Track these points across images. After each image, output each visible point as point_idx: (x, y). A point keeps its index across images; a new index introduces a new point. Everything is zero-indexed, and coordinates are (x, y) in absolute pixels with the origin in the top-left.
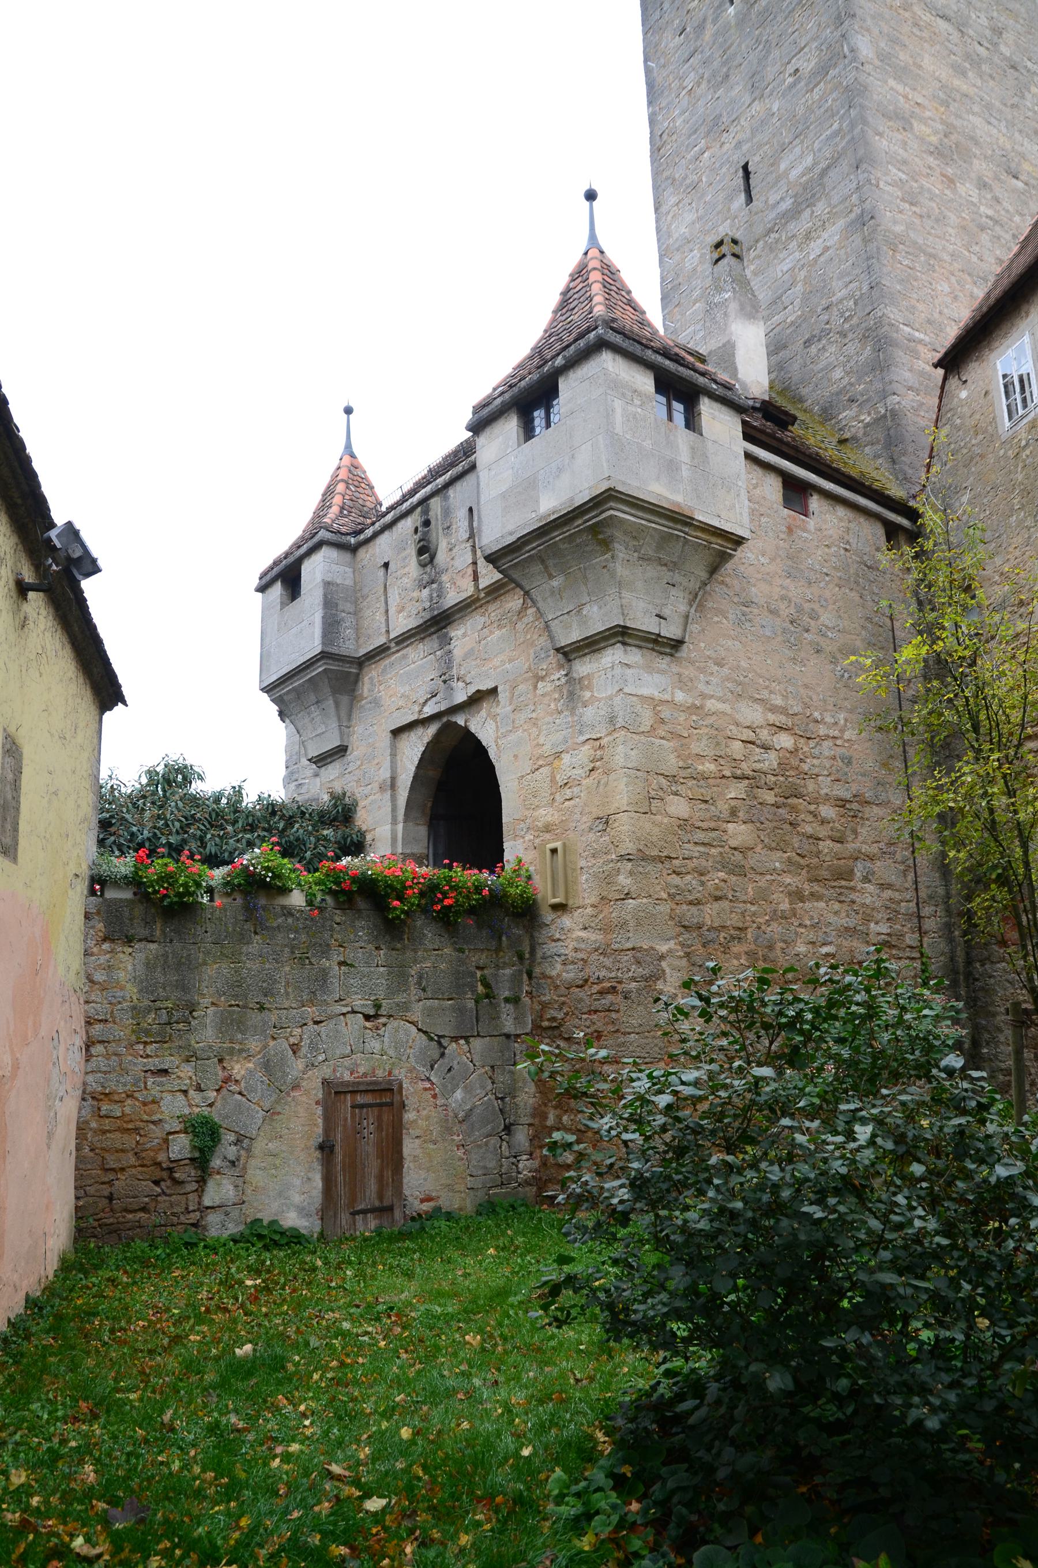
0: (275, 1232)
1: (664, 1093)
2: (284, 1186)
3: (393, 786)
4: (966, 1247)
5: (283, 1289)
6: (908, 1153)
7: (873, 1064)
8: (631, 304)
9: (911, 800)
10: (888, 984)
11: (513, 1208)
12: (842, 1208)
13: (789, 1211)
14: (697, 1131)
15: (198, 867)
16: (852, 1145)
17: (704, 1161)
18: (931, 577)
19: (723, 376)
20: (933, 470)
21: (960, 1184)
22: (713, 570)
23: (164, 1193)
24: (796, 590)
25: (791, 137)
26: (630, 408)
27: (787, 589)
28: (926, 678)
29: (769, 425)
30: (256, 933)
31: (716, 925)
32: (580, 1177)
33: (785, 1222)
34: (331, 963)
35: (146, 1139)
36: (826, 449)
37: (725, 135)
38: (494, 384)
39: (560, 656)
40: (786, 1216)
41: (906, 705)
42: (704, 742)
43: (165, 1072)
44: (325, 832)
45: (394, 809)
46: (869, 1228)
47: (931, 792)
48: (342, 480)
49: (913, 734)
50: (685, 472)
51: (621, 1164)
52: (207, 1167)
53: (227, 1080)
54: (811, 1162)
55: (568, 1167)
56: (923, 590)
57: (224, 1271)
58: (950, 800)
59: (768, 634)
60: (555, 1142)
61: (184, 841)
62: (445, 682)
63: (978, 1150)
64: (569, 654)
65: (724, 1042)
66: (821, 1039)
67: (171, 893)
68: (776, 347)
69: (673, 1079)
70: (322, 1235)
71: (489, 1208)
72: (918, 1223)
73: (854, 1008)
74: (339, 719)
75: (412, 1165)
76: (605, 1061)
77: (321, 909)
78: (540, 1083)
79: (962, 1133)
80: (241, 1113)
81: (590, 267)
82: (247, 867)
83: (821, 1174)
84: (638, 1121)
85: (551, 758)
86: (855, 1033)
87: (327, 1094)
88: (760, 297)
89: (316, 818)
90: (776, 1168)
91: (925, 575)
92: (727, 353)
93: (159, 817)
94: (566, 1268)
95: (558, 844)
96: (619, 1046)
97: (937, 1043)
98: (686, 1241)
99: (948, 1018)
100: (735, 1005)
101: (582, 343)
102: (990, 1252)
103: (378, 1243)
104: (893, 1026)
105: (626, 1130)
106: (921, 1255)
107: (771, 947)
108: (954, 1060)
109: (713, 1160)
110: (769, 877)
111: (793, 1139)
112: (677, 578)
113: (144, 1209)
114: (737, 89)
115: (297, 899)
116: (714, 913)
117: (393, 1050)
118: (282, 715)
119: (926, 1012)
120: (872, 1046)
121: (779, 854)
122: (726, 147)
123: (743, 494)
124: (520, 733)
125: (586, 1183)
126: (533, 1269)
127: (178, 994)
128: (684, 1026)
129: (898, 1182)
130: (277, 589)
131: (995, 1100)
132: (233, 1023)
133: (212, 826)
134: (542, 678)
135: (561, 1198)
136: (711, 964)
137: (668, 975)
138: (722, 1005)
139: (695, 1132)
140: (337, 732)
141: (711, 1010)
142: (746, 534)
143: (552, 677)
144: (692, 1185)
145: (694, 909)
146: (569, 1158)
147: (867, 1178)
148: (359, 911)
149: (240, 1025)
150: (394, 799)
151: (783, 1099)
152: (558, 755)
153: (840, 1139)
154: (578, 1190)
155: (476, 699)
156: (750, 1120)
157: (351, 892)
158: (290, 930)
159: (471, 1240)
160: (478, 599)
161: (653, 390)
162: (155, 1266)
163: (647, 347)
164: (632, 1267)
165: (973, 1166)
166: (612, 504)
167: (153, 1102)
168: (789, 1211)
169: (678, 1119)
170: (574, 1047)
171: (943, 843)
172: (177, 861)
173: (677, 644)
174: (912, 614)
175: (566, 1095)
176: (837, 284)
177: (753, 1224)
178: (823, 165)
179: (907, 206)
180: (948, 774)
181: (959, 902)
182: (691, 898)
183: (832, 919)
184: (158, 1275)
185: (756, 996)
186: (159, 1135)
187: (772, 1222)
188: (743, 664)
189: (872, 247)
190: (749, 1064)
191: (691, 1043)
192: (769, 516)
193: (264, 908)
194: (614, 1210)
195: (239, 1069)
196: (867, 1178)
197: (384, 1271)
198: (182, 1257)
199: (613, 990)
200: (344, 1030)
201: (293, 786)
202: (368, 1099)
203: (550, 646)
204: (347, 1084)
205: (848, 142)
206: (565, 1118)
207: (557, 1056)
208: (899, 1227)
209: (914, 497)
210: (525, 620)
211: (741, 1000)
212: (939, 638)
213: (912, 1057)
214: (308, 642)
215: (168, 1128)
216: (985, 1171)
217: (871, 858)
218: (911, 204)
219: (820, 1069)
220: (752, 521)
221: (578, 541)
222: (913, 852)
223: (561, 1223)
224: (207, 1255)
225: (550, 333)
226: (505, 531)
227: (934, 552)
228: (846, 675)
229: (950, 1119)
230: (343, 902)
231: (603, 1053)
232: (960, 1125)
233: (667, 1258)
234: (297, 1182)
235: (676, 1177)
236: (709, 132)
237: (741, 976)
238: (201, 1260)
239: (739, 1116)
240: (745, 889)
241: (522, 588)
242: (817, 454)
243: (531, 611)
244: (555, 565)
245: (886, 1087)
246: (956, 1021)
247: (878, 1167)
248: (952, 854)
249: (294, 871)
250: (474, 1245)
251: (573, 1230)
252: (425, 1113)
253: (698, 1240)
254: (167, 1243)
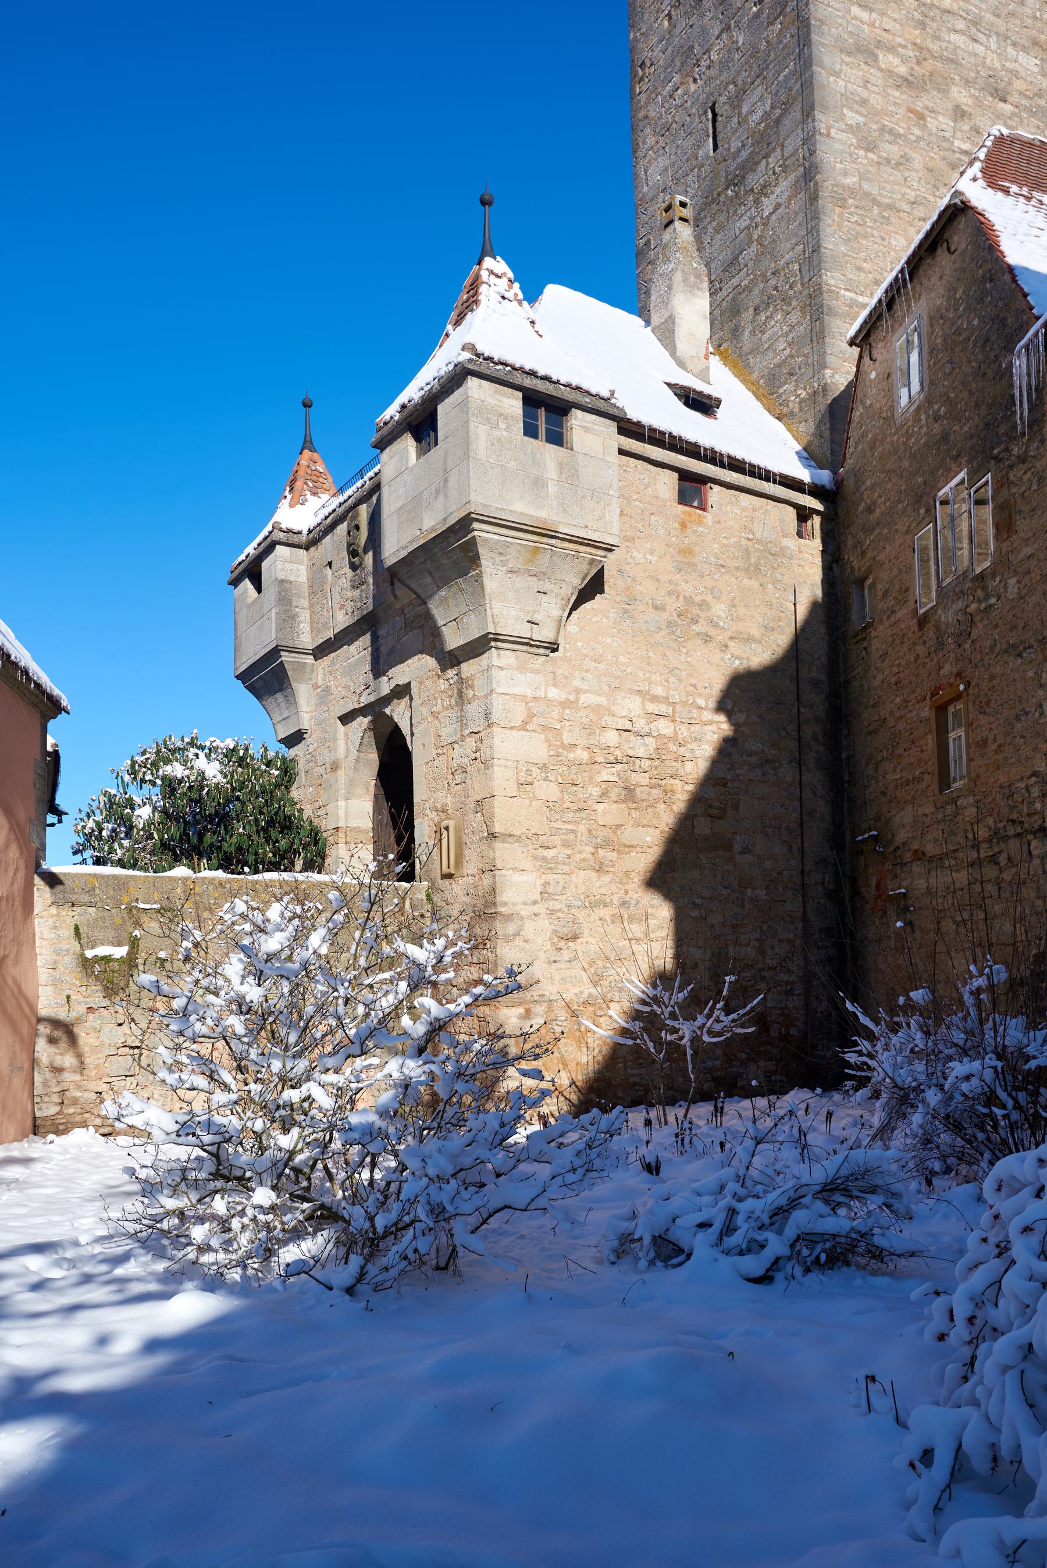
179: (862, 153)
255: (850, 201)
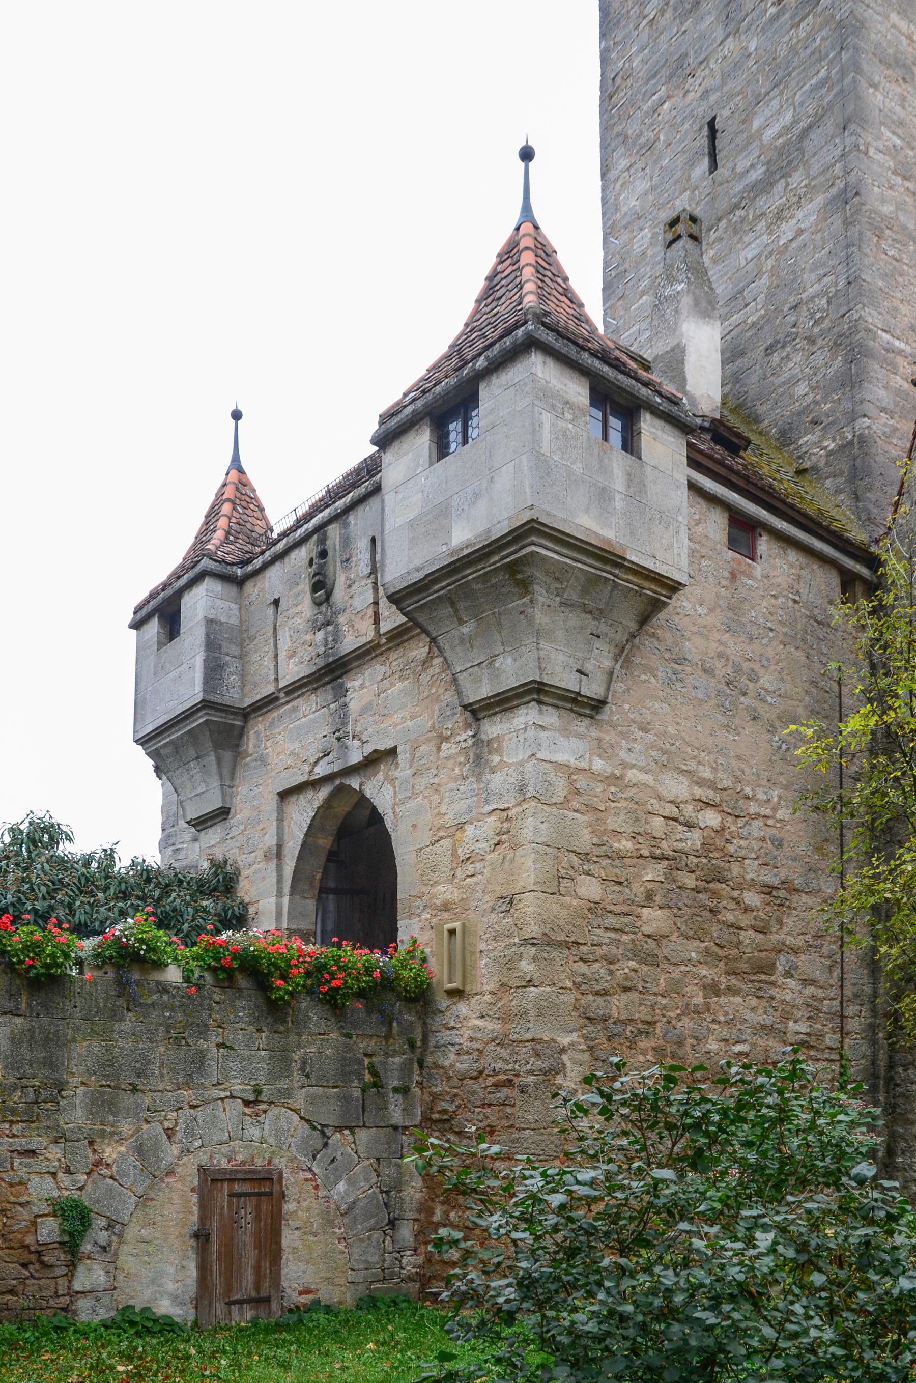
0: (148, 1319)
1: (558, 1192)
2: (159, 1272)
3: (279, 855)
4: (861, 1358)
5: (156, 1376)
6: (809, 1261)
7: (780, 1171)
8: (568, 294)
9: (844, 889)
10: (803, 1087)
11: (395, 1303)
12: (736, 1316)
13: (681, 1316)
14: (590, 1232)
15: (66, 937)
16: (752, 1252)
17: (596, 1262)
18: (888, 637)
19: (669, 388)
20: (902, 510)
21: (861, 1296)
22: (644, 620)
23: (32, 1276)
24: (735, 646)
25: (768, 85)
26: (561, 424)
27: (724, 644)
28: (873, 752)
29: (720, 447)
30: (128, 1010)
31: (623, 1017)
32: (465, 1275)
33: (676, 1327)
34: (209, 1045)
35: (13, 1221)
36: (781, 481)
37: (690, 80)
38: (405, 389)
39: (468, 714)
40: (678, 1321)
41: (847, 782)
42: (622, 817)
43: (32, 1153)
44: (204, 903)
45: (280, 881)
46: (763, 1336)
47: (866, 881)
48: (228, 500)
49: (853, 816)
50: (619, 503)
51: (509, 1263)
52: (77, 1252)
53: (98, 1163)
54: (707, 1267)
55: (454, 1264)
56: (878, 651)
57: (95, 1356)
58: (886, 890)
59: (701, 696)
60: (441, 1239)
61: (52, 908)
62: (339, 739)
63: (883, 1262)
64: (477, 712)
65: (624, 1142)
66: (728, 1142)
67: (38, 964)
68: (732, 353)
69: (568, 1178)
70: (196, 1324)
71: (369, 1303)
72: (813, 1333)
73: (764, 1111)
74: (221, 777)
75: (290, 1257)
76: (497, 1157)
77: (199, 987)
78: (427, 1178)
79: (867, 1244)
80: (113, 1198)
81: (521, 246)
82: (119, 938)
83: (717, 1280)
84: (529, 1220)
85: (453, 830)
86: (764, 1137)
87: (203, 1181)
88: (718, 291)
89: (195, 887)
90: (670, 1272)
91: (882, 634)
92: (675, 359)
93: (23, 880)
94: (447, 1365)
95: (457, 925)
96: (513, 1142)
97: (849, 1150)
98: (573, 1342)
99: (863, 1124)
100: (638, 1103)
101: (508, 341)
102: (885, 1364)
103: (254, 1334)
104: (804, 1131)
105: (516, 1229)
106: (814, 1365)
107: (680, 1044)
108: (866, 1169)
109: (606, 1262)
110: (683, 968)
111: (690, 1244)
112: (603, 628)
113: (11, 1292)
114: (709, 20)
115: (173, 975)
116: (622, 1005)
117: (273, 1137)
118: (158, 770)
119: (841, 1117)
120: (780, 1151)
121: (696, 943)
122: (691, 96)
123: (683, 530)
124: (419, 800)
125: (472, 1281)
126: (413, 1365)
127: (45, 1072)
128: (583, 1124)
129: (797, 1291)
130: (154, 627)
131: (904, 1211)
132: (104, 1104)
133: (81, 892)
134: (447, 739)
135: (445, 1295)
136: (615, 1060)
137: (569, 1070)
138: (624, 1103)
139: (588, 1233)
140: (218, 792)
141: (613, 1108)
142: (683, 579)
143: (458, 738)
144: (582, 1287)
145: (600, 1000)
146: (454, 1255)
147: (764, 1286)
148: (240, 990)
149: (112, 1106)
150: (279, 869)
151: (683, 1203)
152: (461, 826)
153: (739, 1245)
154: (463, 1288)
155: (373, 761)
156: (646, 1223)
157: (233, 970)
158: (165, 1007)
159: (350, 1334)
160: (378, 645)
161: (587, 402)
162: (23, 1349)
163: (583, 348)
164: (515, 1366)
165: (876, 1278)
166: (534, 538)
167: (21, 1183)
168: (681, 1316)
169: (570, 1220)
170: (465, 1142)
171: (875, 937)
172: (44, 929)
173: (598, 705)
174: (862, 679)
175: (453, 1191)
176: (809, 277)
177: (643, 1328)
178: (803, 124)
180: (887, 862)
181: (886, 1002)
182: (597, 988)
183: (749, 1015)
184: (27, 1358)
185: (661, 1095)
186: (27, 1217)
187: (663, 1326)
188: (671, 730)
189: (854, 231)
190: (649, 1165)
191: (589, 1142)
192: (710, 558)
193: (138, 983)
194: (500, 1309)
195: (110, 1152)
196: (765, 1286)
197: (259, 1361)
198: (52, 1341)
199: (509, 1083)
200: (222, 1115)
201: (169, 851)
202: (246, 1188)
203: (456, 702)
204: (225, 1172)
205: (835, 96)
206: (452, 1214)
207: (446, 1150)
208: (795, 1336)
209: (877, 541)
210: (431, 671)
211: (645, 1098)
212: (890, 708)
213: (822, 1164)
214: (187, 687)
215: (35, 1210)
216: (888, 1282)
217: (795, 951)
218: (905, 178)
219: (724, 1173)
220: (691, 563)
221: (494, 581)
222: (841, 946)
223: (444, 1321)
224: (77, 1340)
225: (471, 327)
226: (411, 567)
227: (893, 607)
228: (784, 746)
229: (856, 1228)
230: (223, 980)
231: (496, 1149)
232: (867, 1235)
233: (553, 1359)
234: (171, 1270)
235: (566, 1278)
236: (671, 77)
237: (647, 1073)
238: (71, 1344)
239: (636, 1218)
240: (656, 981)
241: (428, 634)
242: (771, 486)
243: (437, 661)
244: (466, 609)
245: (792, 1194)
246: (872, 1128)
247: (777, 1275)
248: (883, 950)
249: (170, 944)
250: (353, 1339)
251: (456, 1328)
252: (305, 1204)
253: (584, 1341)
254: (35, 1326)
255: (888, 232)
